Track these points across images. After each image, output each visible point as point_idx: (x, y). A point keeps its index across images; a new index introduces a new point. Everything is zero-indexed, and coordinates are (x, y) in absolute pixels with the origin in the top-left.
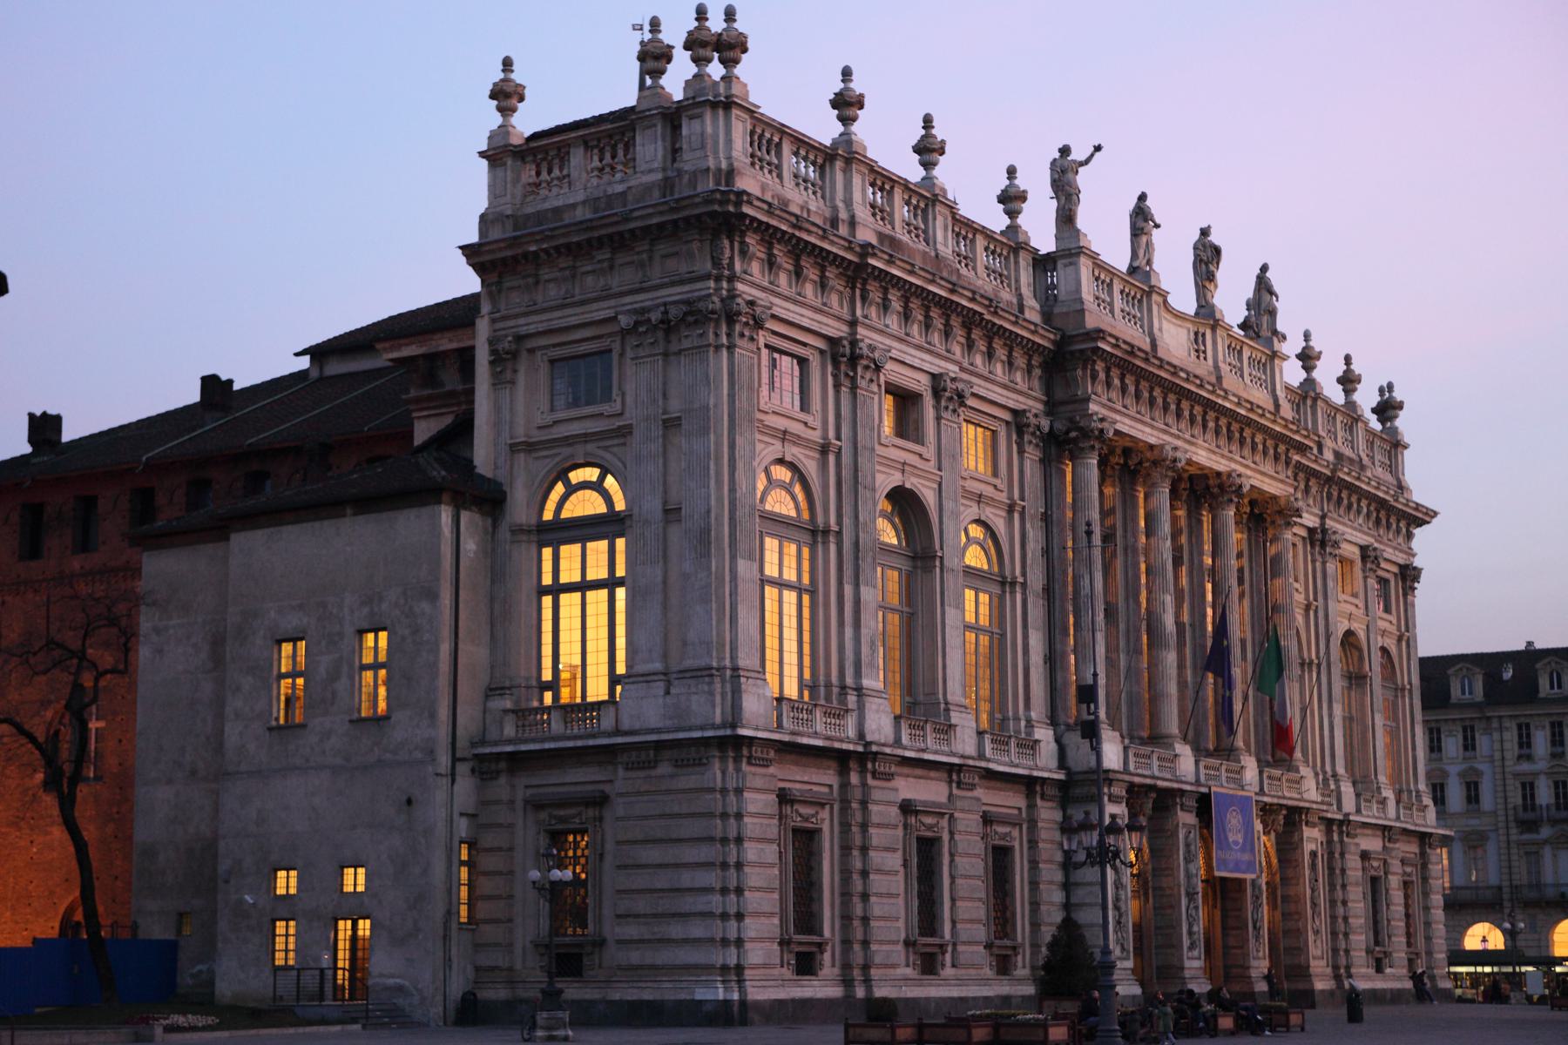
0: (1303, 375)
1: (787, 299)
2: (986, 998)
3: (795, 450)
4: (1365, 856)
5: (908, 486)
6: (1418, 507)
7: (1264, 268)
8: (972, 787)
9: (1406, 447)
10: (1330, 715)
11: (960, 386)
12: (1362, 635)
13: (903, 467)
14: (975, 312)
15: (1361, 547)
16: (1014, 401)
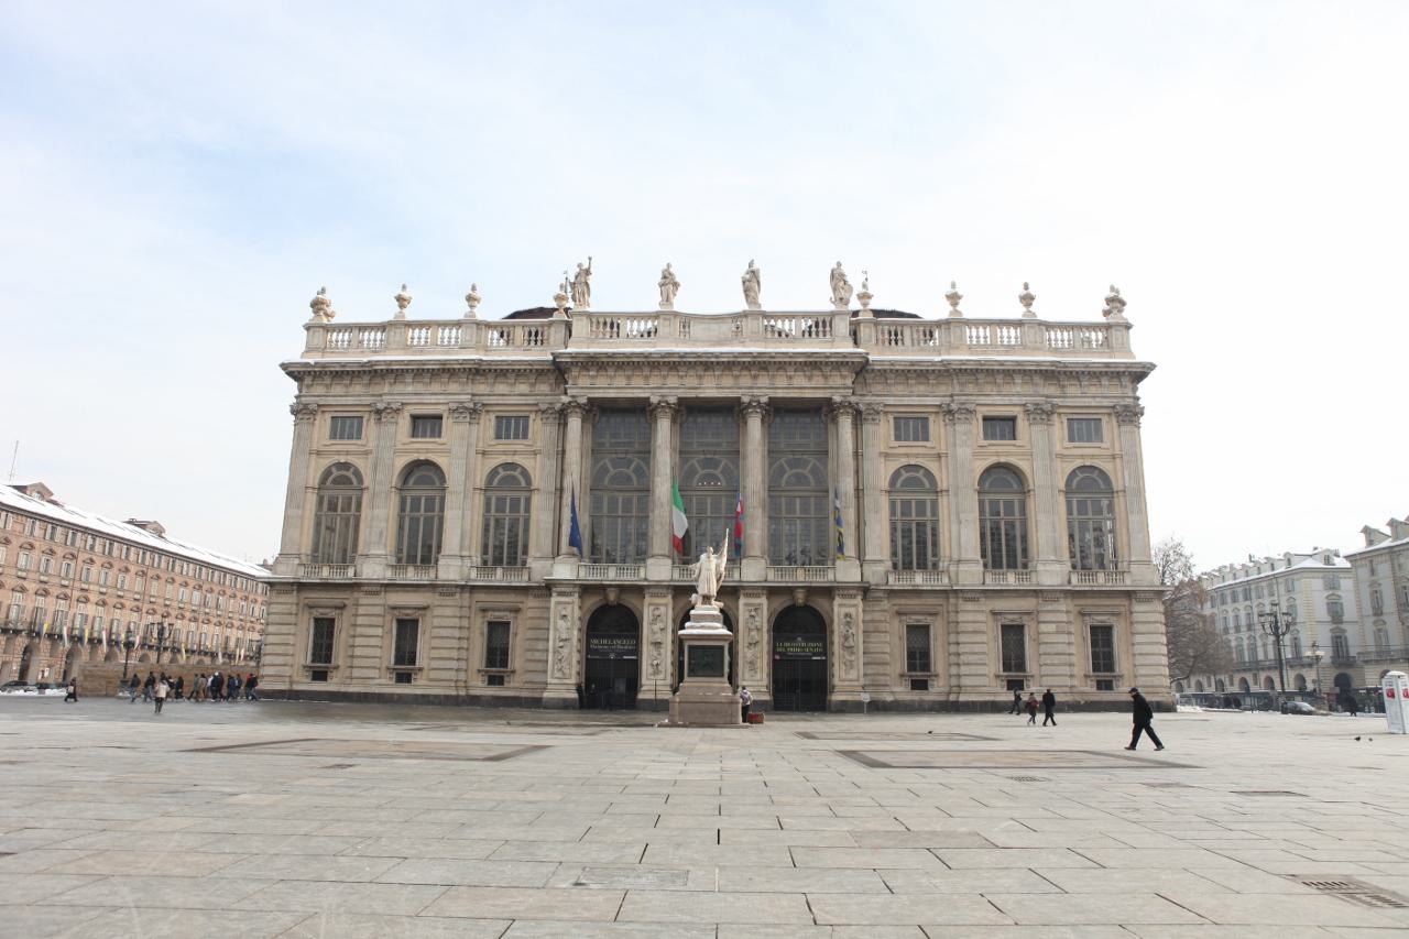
0: (951, 308)
1: (335, 396)
2: (446, 696)
3: (349, 457)
4: (994, 613)
5: (422, 457)
6: (1143, 365)
7: (839, 264)
8: (452, 594)
9: (1128, 327)
10: (960, 523)
11: (466, 405)
12: (1023, 465)
13: (417, 451)
14: (470, 369)
15: (1024, 405)
16: (531, 400)
